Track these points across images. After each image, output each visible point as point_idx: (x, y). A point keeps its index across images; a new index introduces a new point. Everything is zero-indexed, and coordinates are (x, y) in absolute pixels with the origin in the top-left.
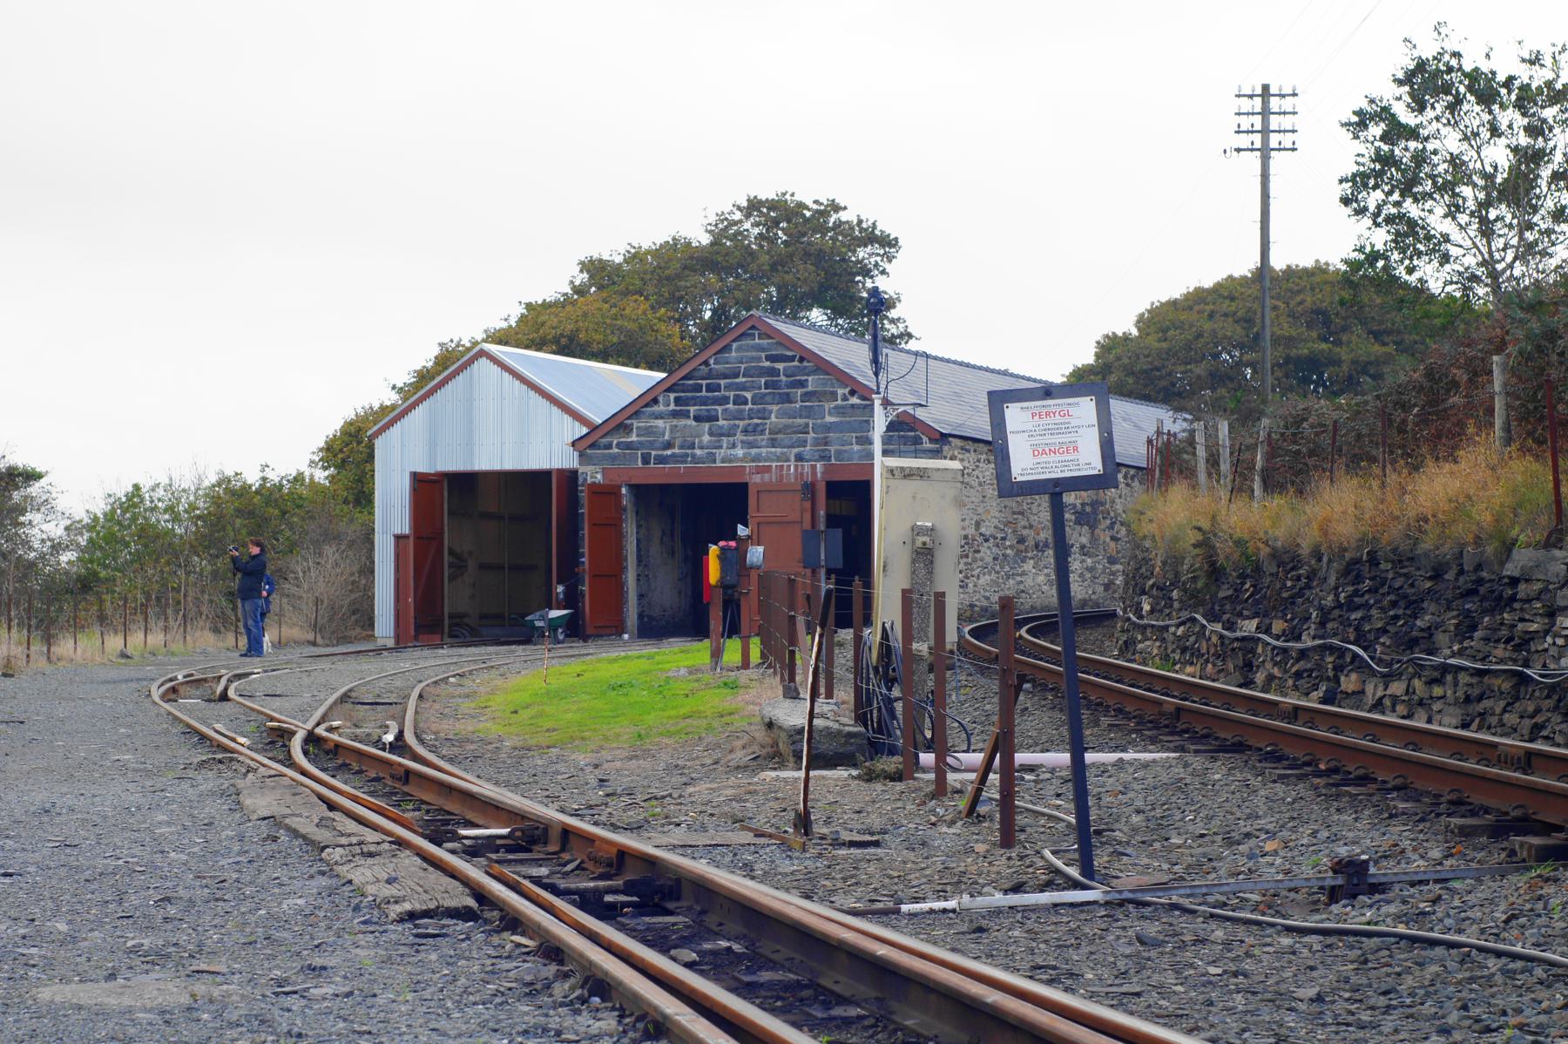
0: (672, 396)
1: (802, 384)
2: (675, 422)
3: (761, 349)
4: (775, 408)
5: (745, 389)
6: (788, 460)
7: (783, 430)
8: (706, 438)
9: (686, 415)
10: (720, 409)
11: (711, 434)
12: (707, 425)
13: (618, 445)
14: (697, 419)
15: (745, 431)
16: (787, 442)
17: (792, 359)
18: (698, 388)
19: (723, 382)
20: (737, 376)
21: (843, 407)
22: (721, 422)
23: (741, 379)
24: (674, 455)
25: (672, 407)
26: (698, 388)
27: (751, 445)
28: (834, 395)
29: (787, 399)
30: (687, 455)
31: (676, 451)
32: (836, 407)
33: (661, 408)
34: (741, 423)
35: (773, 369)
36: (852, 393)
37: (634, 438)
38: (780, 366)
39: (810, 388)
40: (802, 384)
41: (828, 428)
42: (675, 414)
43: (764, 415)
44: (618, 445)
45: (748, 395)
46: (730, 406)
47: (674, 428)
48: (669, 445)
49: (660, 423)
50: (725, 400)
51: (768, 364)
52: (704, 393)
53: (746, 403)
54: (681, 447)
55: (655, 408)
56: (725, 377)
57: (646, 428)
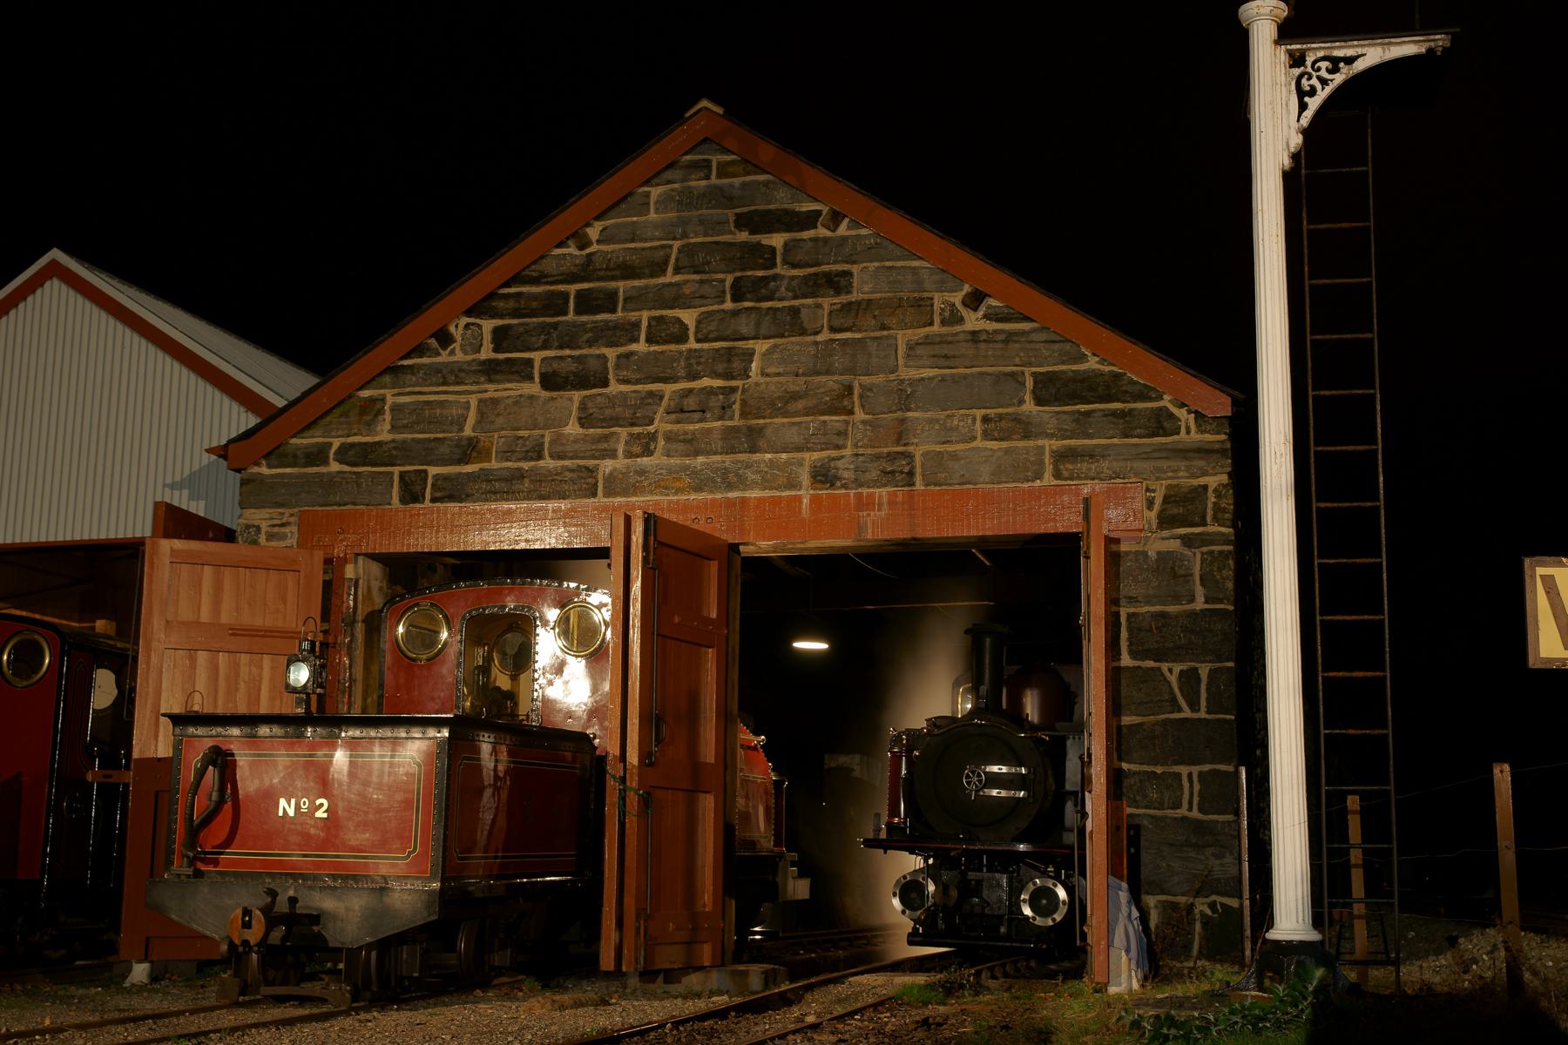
0: (488, 325)
1: (836, 283)
2: (492, 390)
3: (724, 198)
4: (761, 346)
5: (679, 300)
6: (793, 484)
7: (784, 404)
8: (572, 429)
9: (522, 371)
10: (611, 353)
11: (584, 421)
12: (577, 396)
13: (344, 454)
14: (549, 382)
15: (679, 411)
16: (792, 436)
17: (810, 220)
18: (556, 304)
19: (622, 286)
20: (659, 268)
21: (942, 340)
22: (614, 388)
23: (670, 278)
24: (485, 476)
25: (486, 353)
26: (556, 304)
27: (693, 445)
28: (921, 308)
29: (793, 323)
30: (520, 475)
31: (494, 464)
32: (927, 341)
33: (456, 355)
34: (669, 389)
35: (758, 247)
36: (974, 300)
37: (383, 433)
38: (777, 240)
39: (855, 296)
40: (836, 283)
41: (904, 397)
42: (491, 370)
43: (733, 364)
44: (344, 454)
45: (689, 317)
46: (641, 347)
47: (488, 408)
48: (469, 451)
49: (451, 395)
50: (629, 332)
51: (744, 236)
52: (571, 316)
53: (682, 338)
54: (506, 454)
55: (444, 357)
56: (628, 272)
57: (417, 408)
